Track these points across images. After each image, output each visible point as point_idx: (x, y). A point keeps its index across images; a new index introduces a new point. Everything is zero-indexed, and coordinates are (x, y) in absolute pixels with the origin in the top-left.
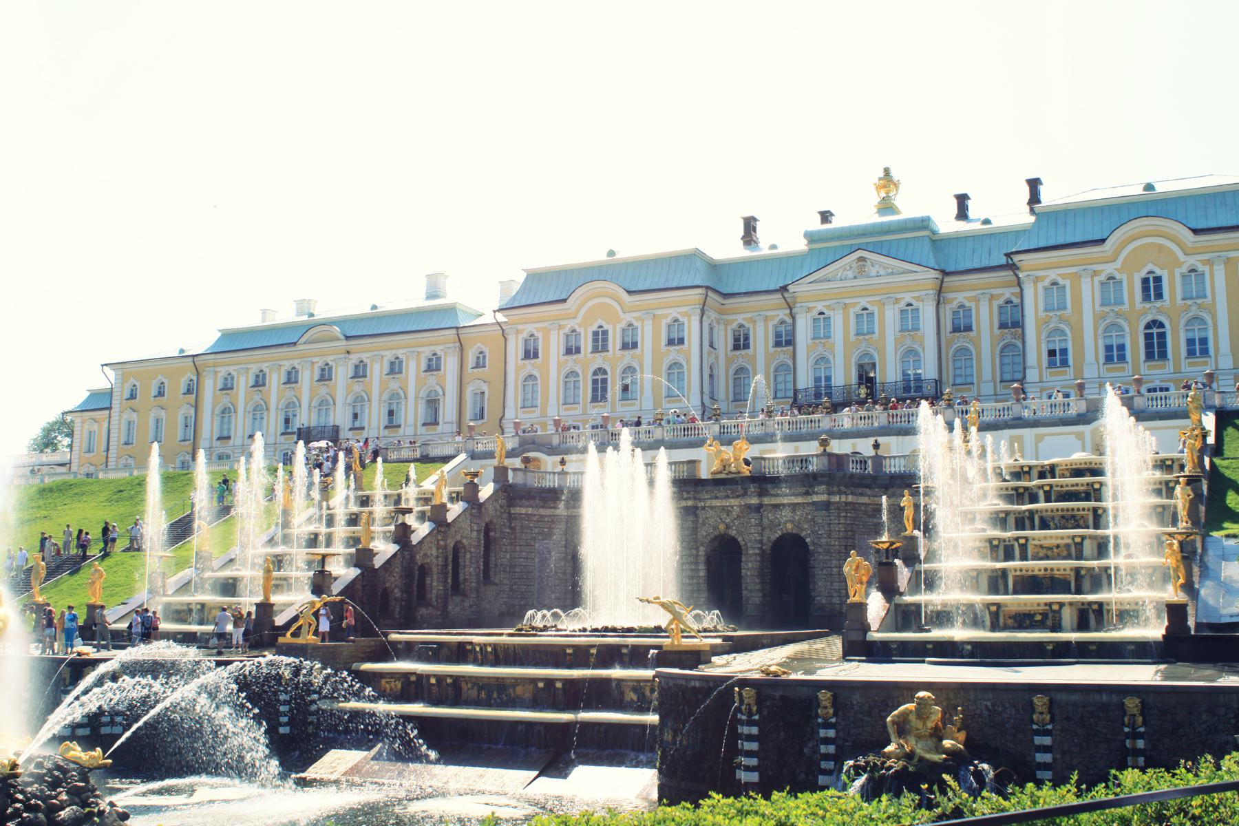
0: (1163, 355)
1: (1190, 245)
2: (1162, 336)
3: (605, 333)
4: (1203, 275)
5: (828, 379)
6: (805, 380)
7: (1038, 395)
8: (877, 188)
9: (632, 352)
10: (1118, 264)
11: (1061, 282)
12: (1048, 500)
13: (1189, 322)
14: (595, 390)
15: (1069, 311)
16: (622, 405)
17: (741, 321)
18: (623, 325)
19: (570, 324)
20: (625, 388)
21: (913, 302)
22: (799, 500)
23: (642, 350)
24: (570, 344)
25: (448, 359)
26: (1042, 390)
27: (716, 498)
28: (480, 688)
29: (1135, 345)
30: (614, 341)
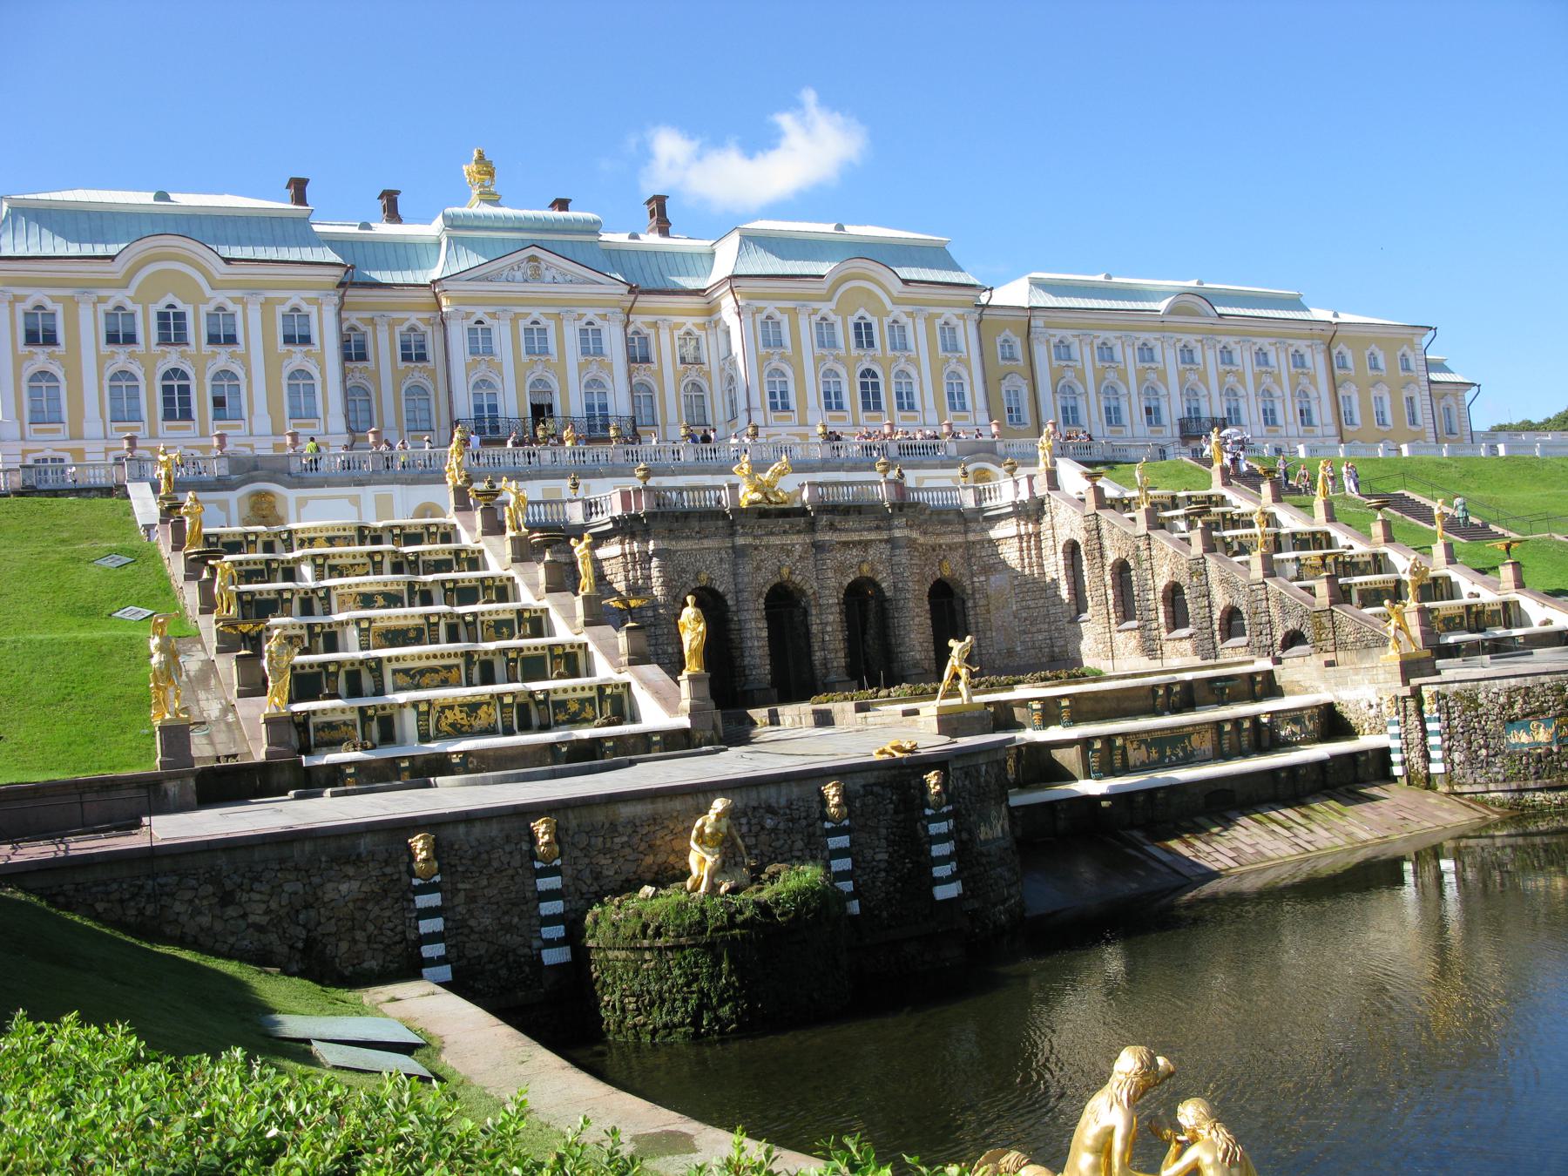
0: (878, 407)
1: (895, 294)
2: (876, 386)
3: (180, 316)
4: (903, 328)
5: (493, 408)
9: (231, 349)
10: (832, 305)
11: (778, 316)
13: (897, 376)
14: (168, 402)
17: (353, 321)
18: (211, 308)
20: (219, 402)
21: (598, 323)
22: (872, 536)
24: (112, 329)
27: (772, 534)
28: (1149, 747)
29: (851, 394)
30: (196, 330)
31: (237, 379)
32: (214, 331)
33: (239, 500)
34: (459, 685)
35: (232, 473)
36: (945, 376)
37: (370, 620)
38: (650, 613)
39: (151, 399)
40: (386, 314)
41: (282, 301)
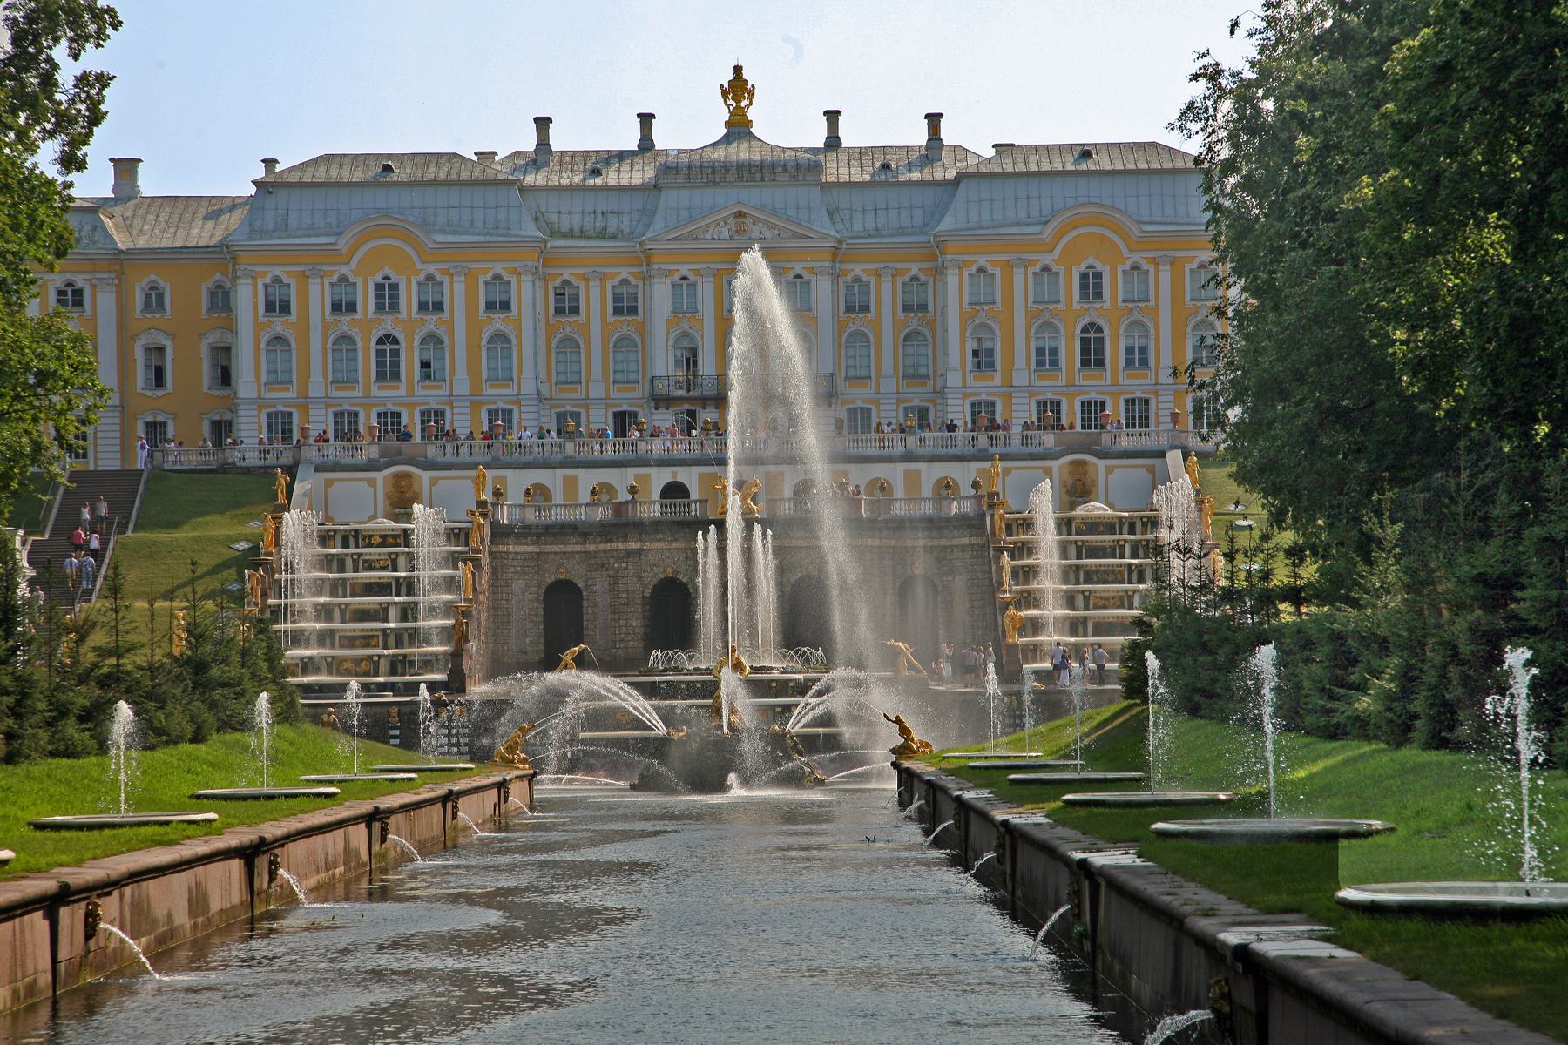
0: (1100, 363)
2: (1100, 341)
3: (394, 287)
6: (664, 365)
7: (960, 402)
8: (725, 94)
10: (1056, 254)
12: (1079, 557)
14: (380, 364)
15: (998, 306)
16: (423, 388)
17: (566, 276)
18: (422, 278)
19: (344, 270)
20: (425, 365)
23: (452, 315)
24: (337, 298)
25: (99, 296)
26: (965, 396)
29: (1070, 352)
30: (409, 298)
31: (442, 343)
32: (423, 299)
33: (385, 478)
34: (376, 646)
35: (381, 456)
36: (1189, 330)
37: (346, 604)
38: (624, 596)
39: (367, 362)
40: (598, 269)
41: (485, 271)
